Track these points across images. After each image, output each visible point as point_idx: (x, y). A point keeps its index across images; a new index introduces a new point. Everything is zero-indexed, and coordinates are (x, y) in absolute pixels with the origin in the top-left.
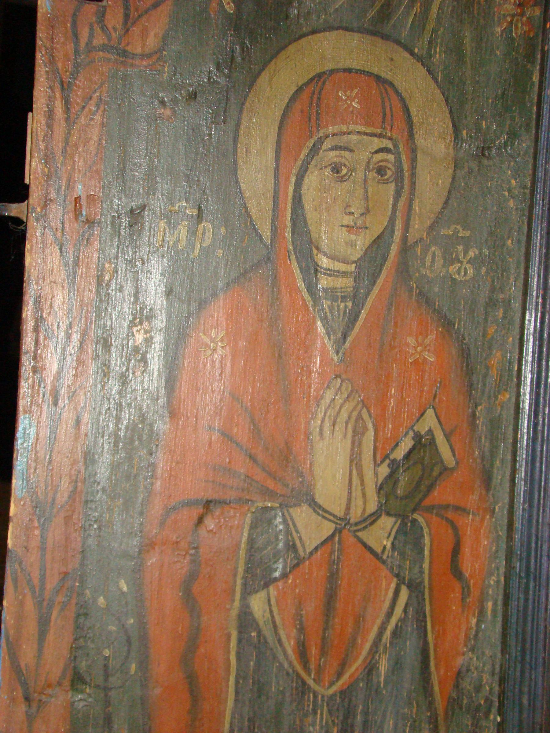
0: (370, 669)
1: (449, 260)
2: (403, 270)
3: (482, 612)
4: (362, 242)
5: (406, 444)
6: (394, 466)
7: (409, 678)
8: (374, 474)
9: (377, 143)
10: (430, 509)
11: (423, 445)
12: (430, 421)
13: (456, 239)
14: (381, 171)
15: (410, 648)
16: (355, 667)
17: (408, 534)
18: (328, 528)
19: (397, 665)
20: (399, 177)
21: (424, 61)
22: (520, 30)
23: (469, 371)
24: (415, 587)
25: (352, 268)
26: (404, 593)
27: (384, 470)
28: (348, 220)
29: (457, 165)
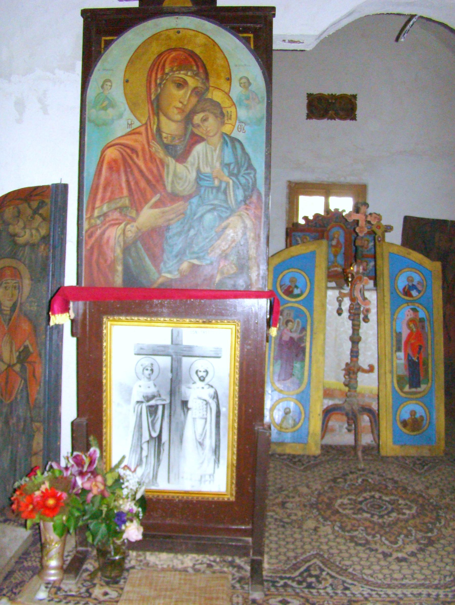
0: (16, 398)
1: (31, 306)
2: (21, 309)
3: (40, 385)
4: (12, 303)
5: (22, 348)
6: (20, 353)
7: (24, 401)
8: (16, 355)
9: (14, 281)
10: (28, 362)
11: (26, 347)
12: (27, 343)
13: (32, 301)
14: (15, 287)
15: (25, 394)
16: (13, 397)
17: (23, 368)
18: (6, 366)
19: (22, 397)
20: (19, 289)
21: (24, 263)
22: (45, 255)
23: (36, 331)
24: (25, 380)
25: (9, 309)
26: (23, 381)
27: (18, 354)
28: (9, 299)
29: (32, 285)
